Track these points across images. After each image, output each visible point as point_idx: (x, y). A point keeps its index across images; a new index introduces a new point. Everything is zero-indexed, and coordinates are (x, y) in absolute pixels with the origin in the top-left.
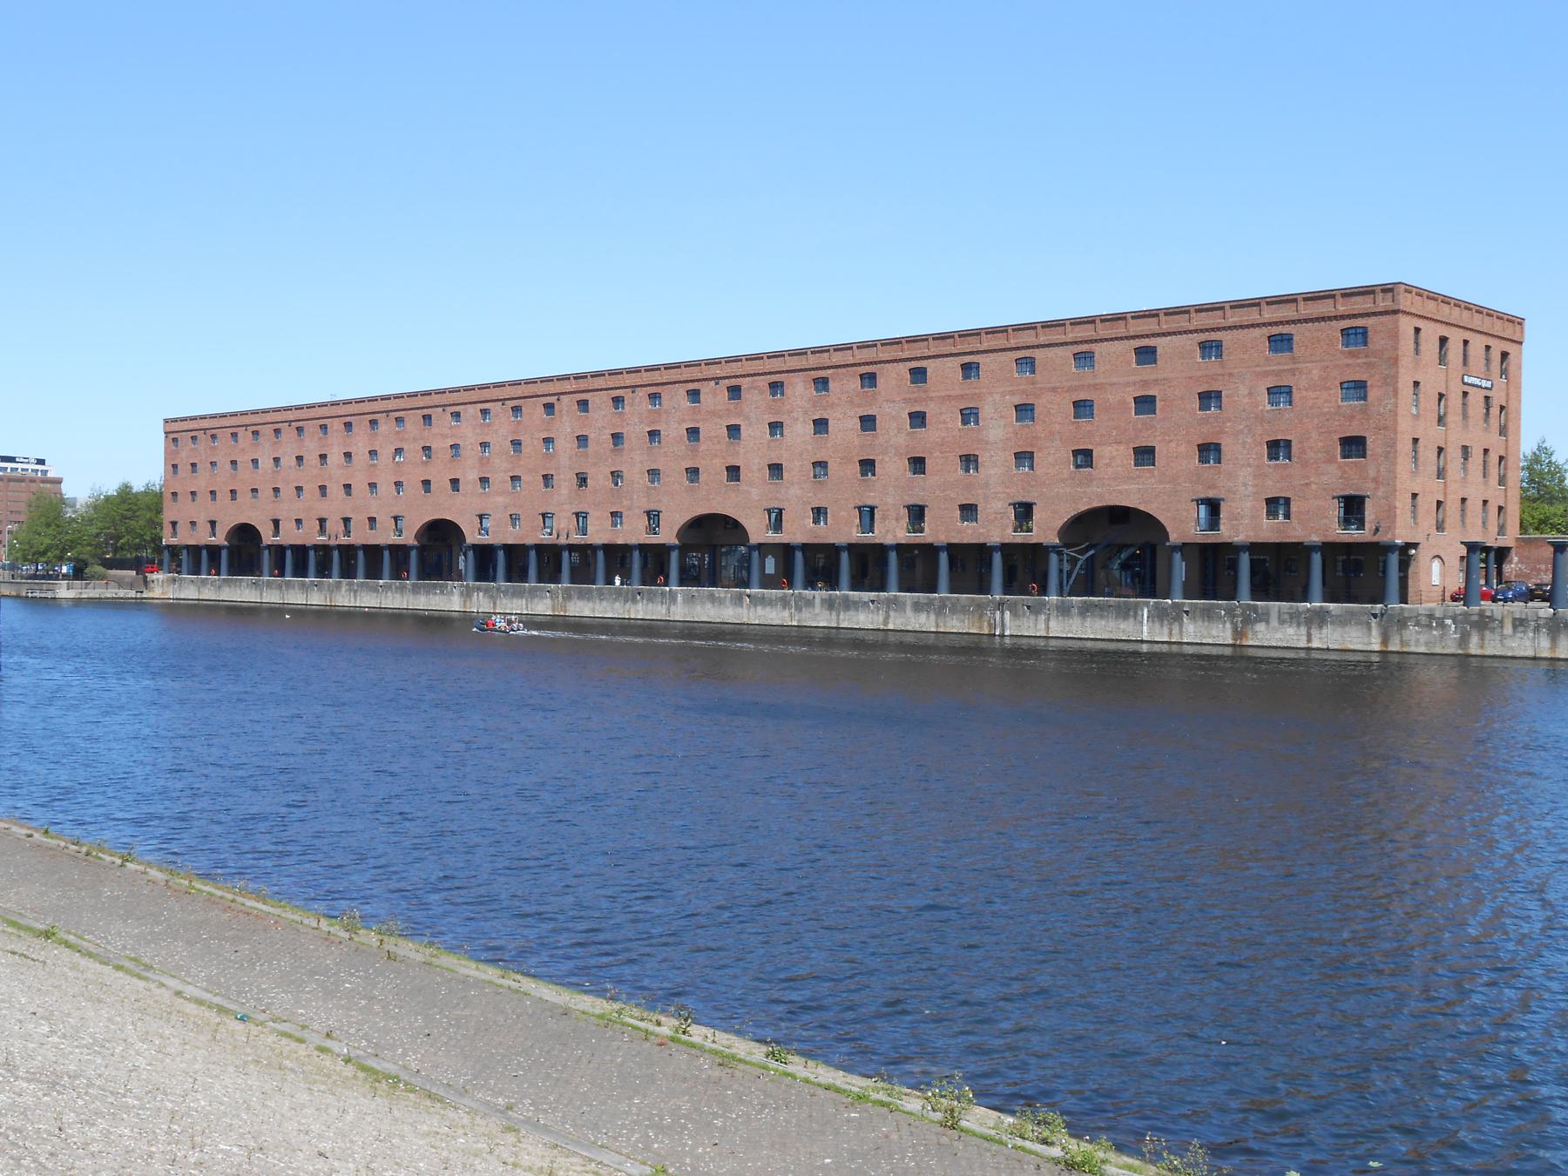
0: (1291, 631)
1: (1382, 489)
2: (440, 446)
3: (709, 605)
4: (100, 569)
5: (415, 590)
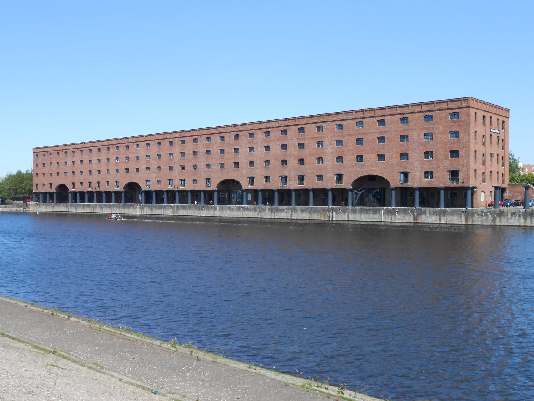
0: (434, 217)
1: (465, 168)
2: (132, 156)
3: (228, 211)
4: (10, 201)
5: (124, 207)
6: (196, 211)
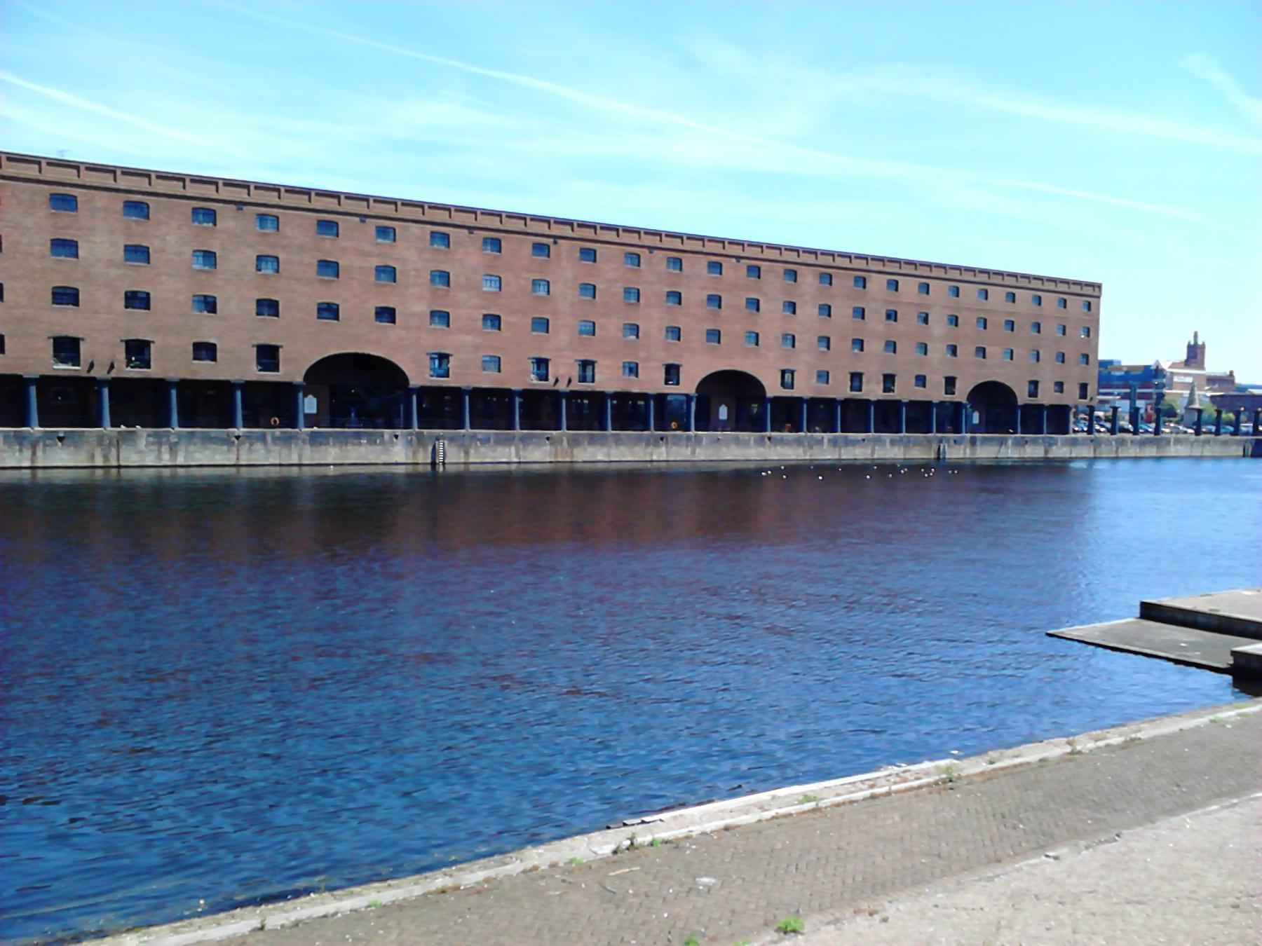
3: (733, 447)
6: (637, 449)
